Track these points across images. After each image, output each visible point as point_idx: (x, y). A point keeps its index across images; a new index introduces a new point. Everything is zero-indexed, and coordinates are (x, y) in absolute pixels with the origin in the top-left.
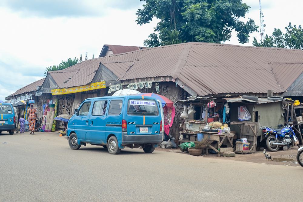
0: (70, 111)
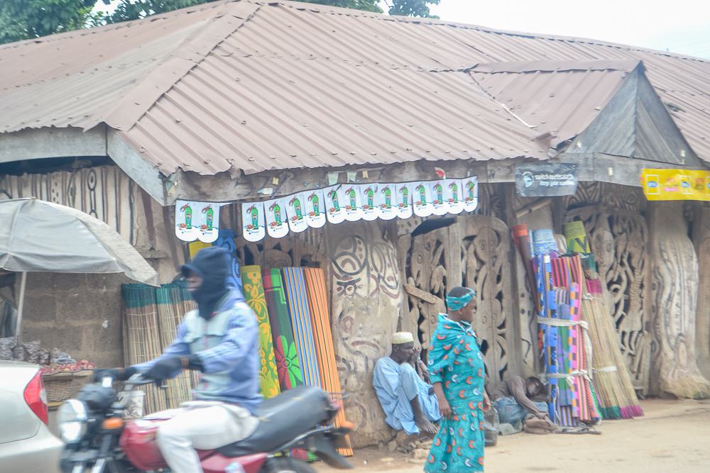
0: (627, 292)
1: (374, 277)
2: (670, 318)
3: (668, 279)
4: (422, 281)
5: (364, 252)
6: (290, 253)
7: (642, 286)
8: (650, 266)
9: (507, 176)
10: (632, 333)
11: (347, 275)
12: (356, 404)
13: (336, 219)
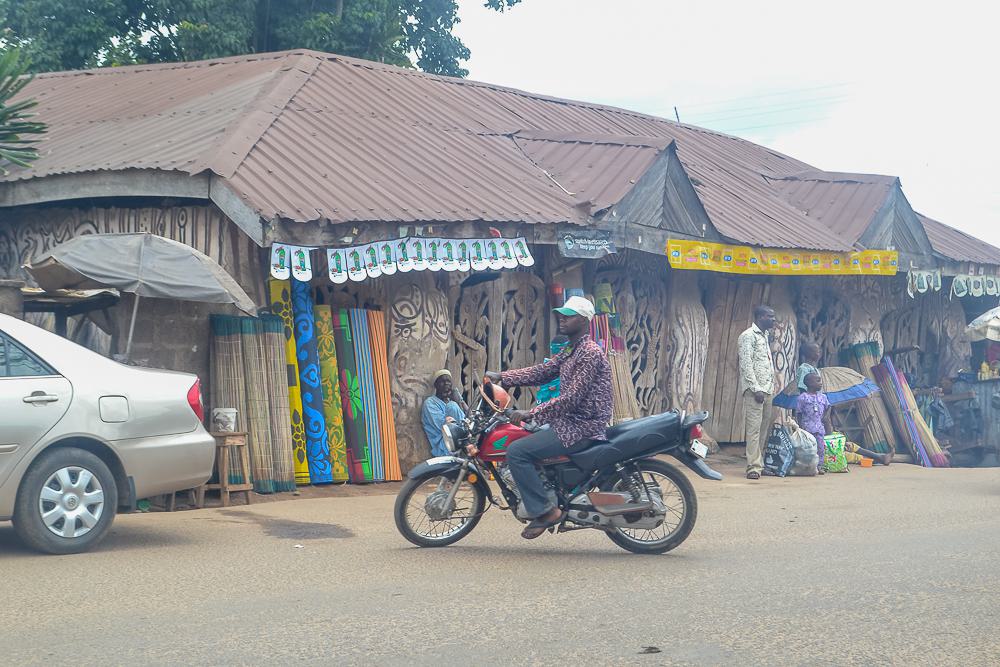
1: (428, 322)
2: (681, 378)
3: (682, 343)
4: (468, 329)
5: (420, 300)
6: (356, 296)
7: (658, 347)
8: (666, 329)
9: (551, 239)
10: (646, 389)
11: (404, 319)
12: (406, 436)
13: (405, 268)
